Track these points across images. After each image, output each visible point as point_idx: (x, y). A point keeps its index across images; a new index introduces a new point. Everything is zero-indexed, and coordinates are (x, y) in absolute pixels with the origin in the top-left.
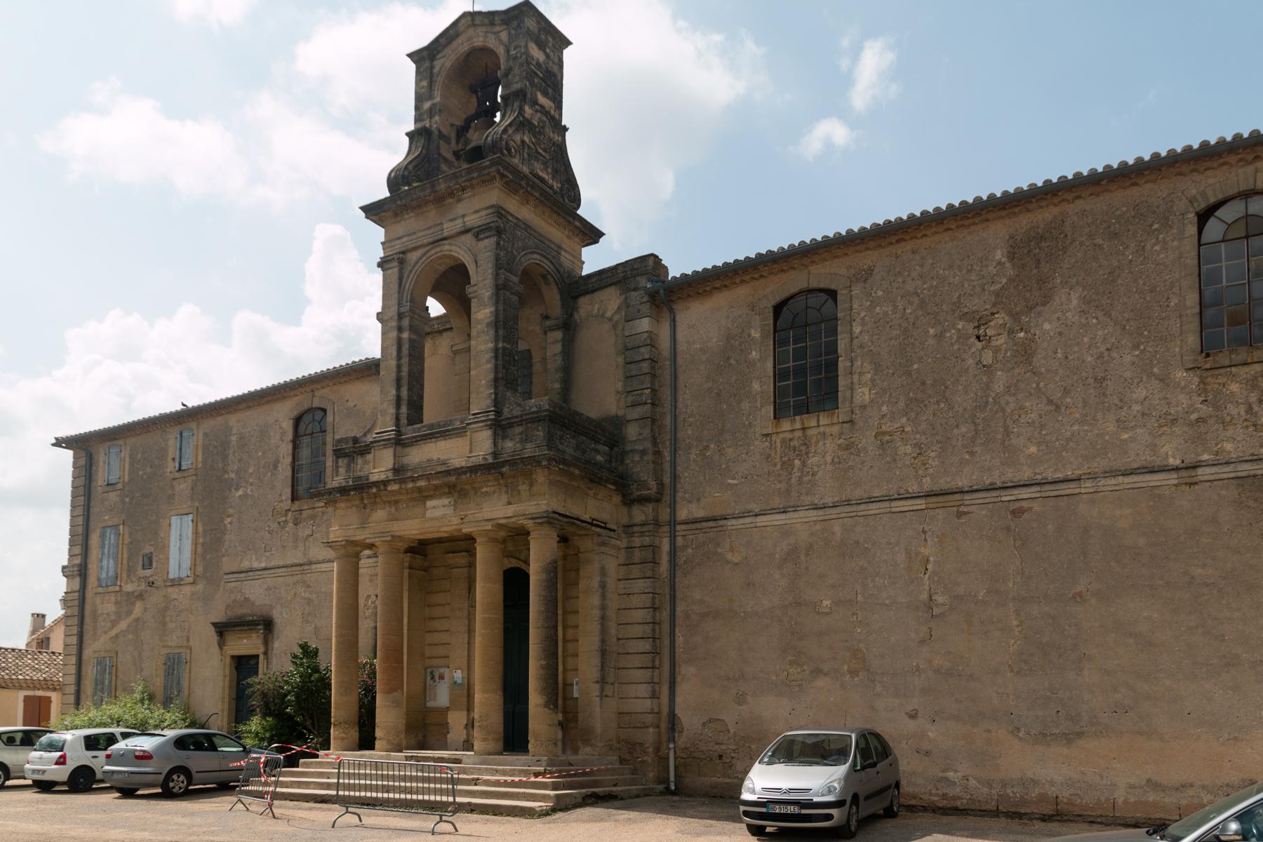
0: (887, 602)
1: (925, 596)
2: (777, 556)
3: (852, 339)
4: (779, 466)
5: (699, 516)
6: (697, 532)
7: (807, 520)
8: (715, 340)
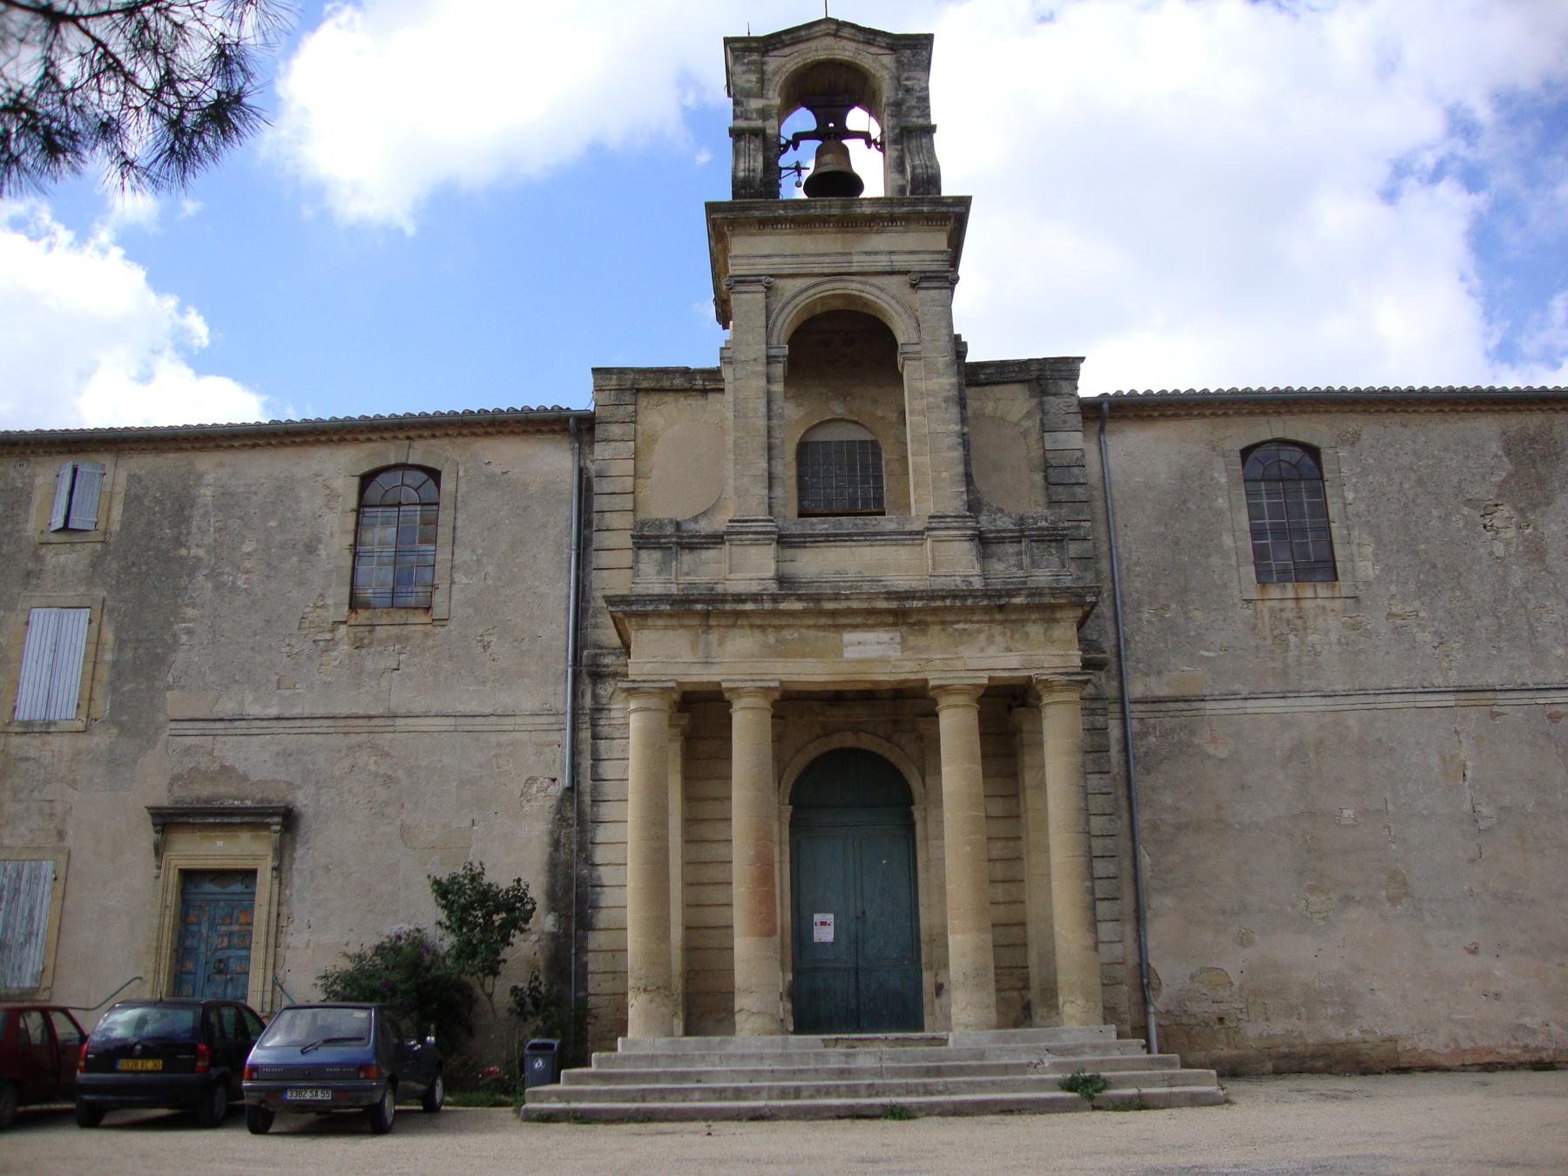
0: (1425, 813)
2: (1278, 752)
3: (1345, 505)
4: (1269, 641)
6: (1161, 715)
7: (1313, 709)
8: (1163, 476)
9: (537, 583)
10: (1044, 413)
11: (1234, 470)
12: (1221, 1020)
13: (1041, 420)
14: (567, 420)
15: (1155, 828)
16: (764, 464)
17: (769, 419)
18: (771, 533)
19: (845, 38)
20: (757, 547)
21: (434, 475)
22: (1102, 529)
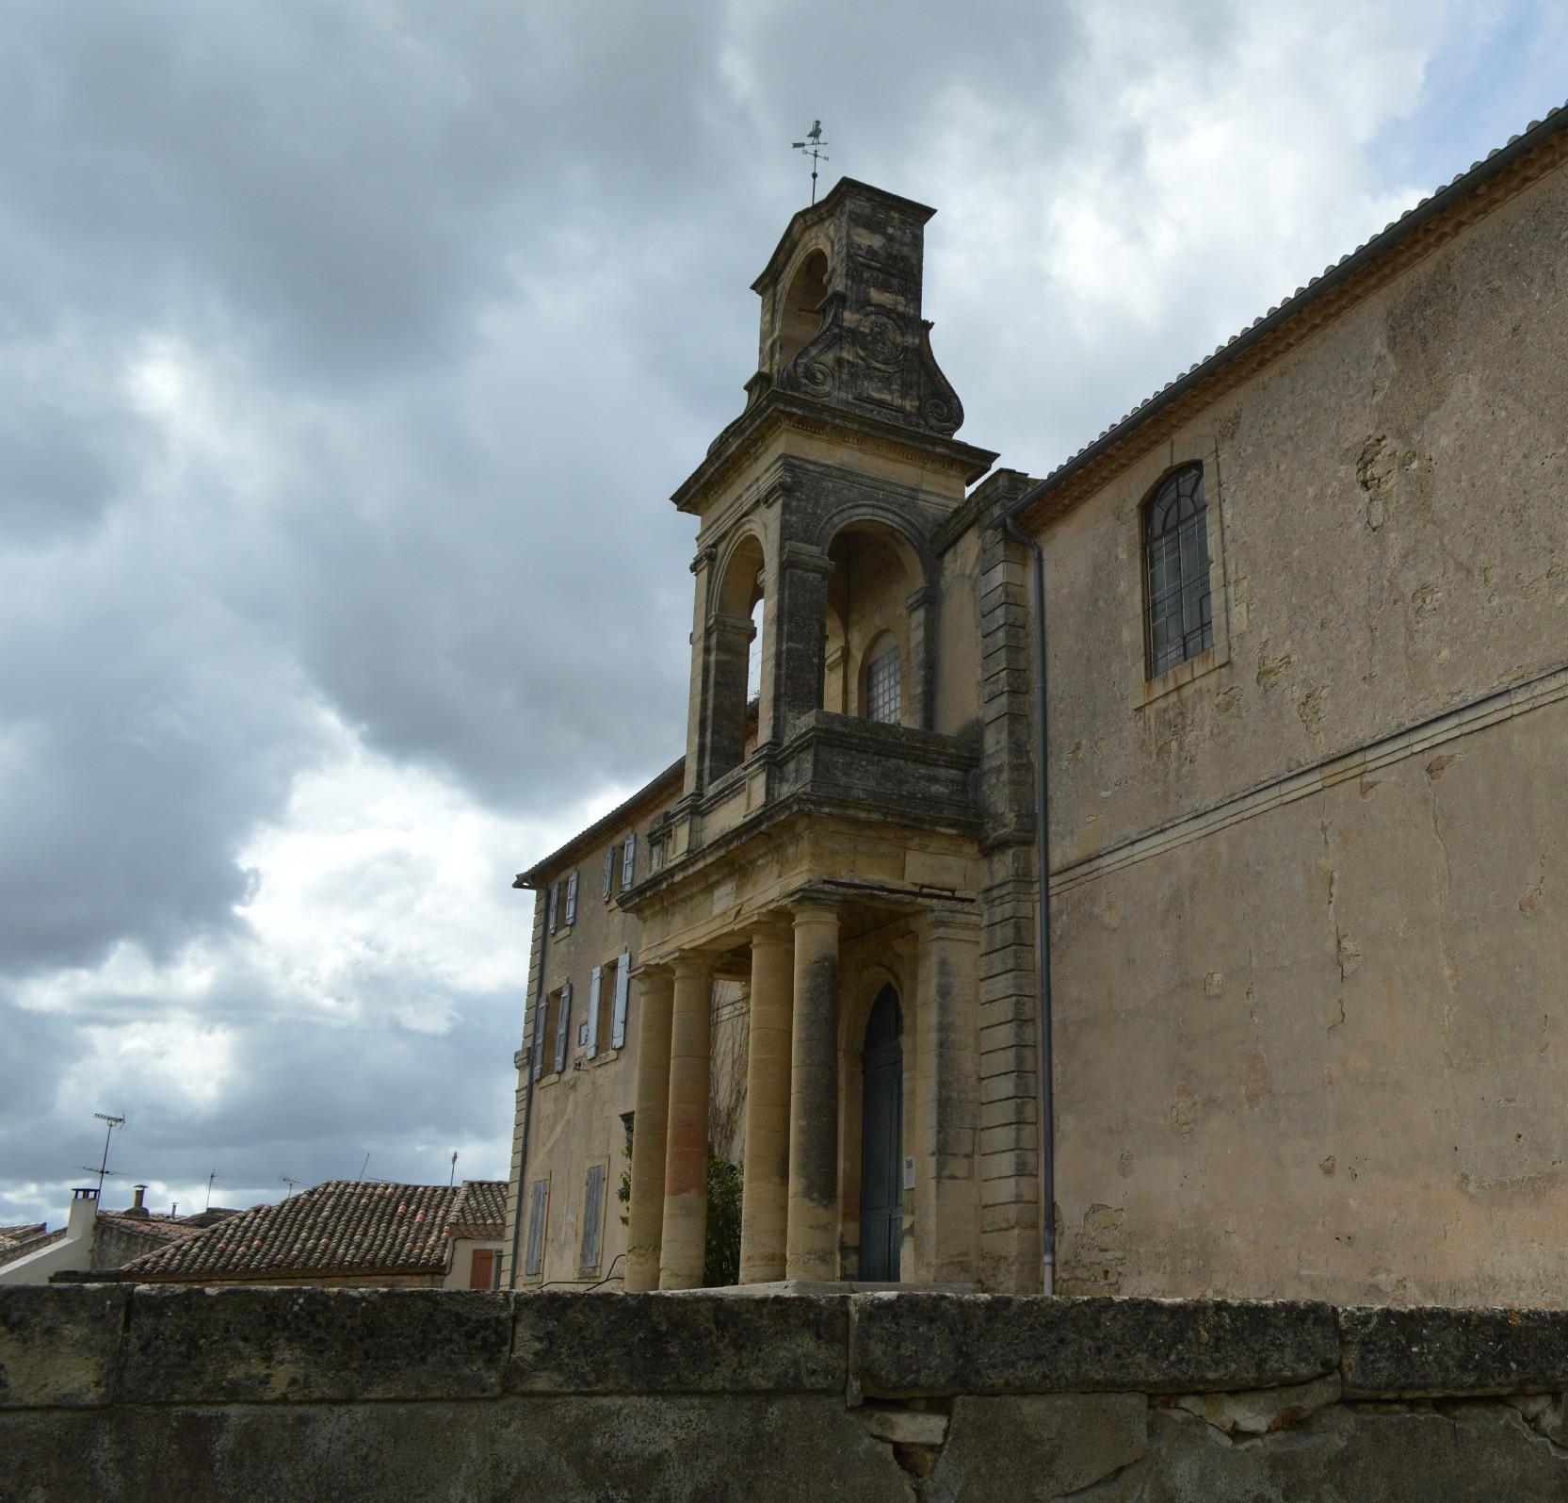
0: (1287, 963)
1: (1331, 945)
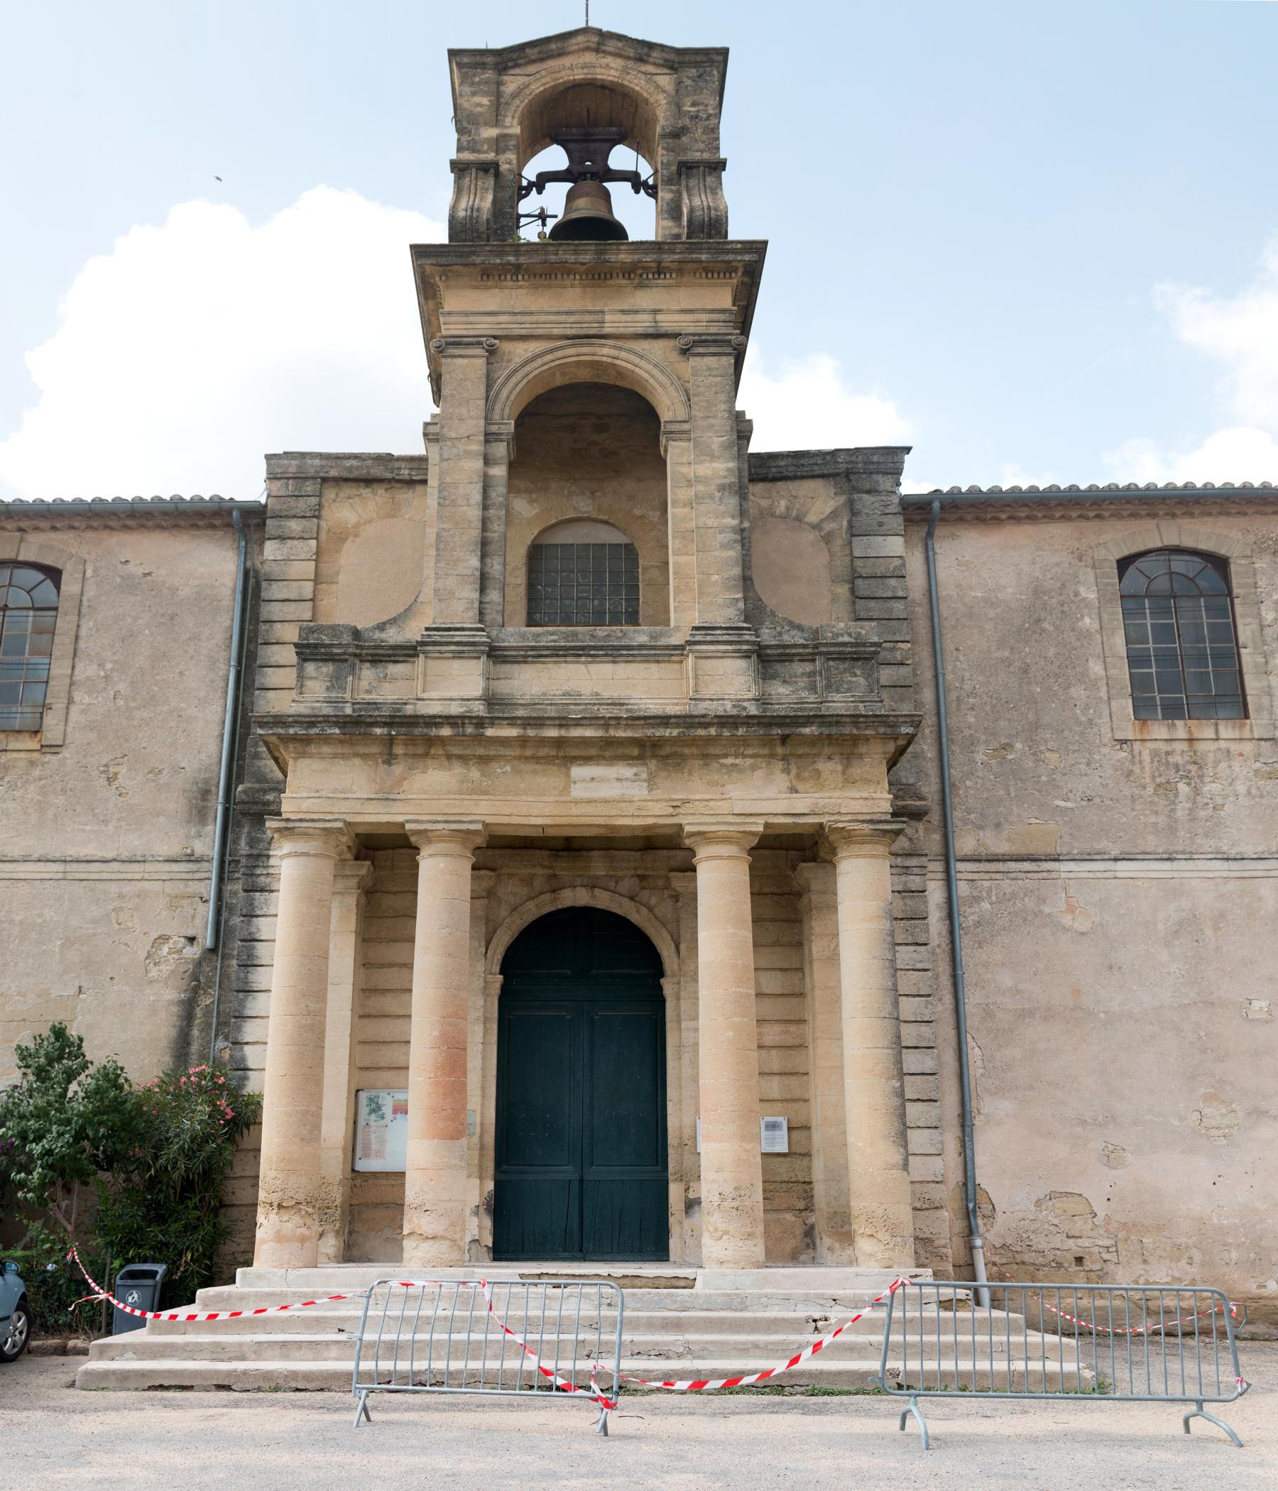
2: (1160, 927)
3: (1262, 627)
4: (1150, 790)
5: (1001, 851)
6: (998, 876)
7: (1211, 875)
8: (1010, 590)
9: (183, 705)
10: (854, 513)
11: (1109, 584)
12: (1079, 1260)
13: (850, 522)
14: (230, 512)
15: (988, 1013)
16: (475, 562)
17: (485, 508)
18: (482, 644)
19: (610, 54)
20: (460, 661)
21: (54, 574)
22: (924, 653)
